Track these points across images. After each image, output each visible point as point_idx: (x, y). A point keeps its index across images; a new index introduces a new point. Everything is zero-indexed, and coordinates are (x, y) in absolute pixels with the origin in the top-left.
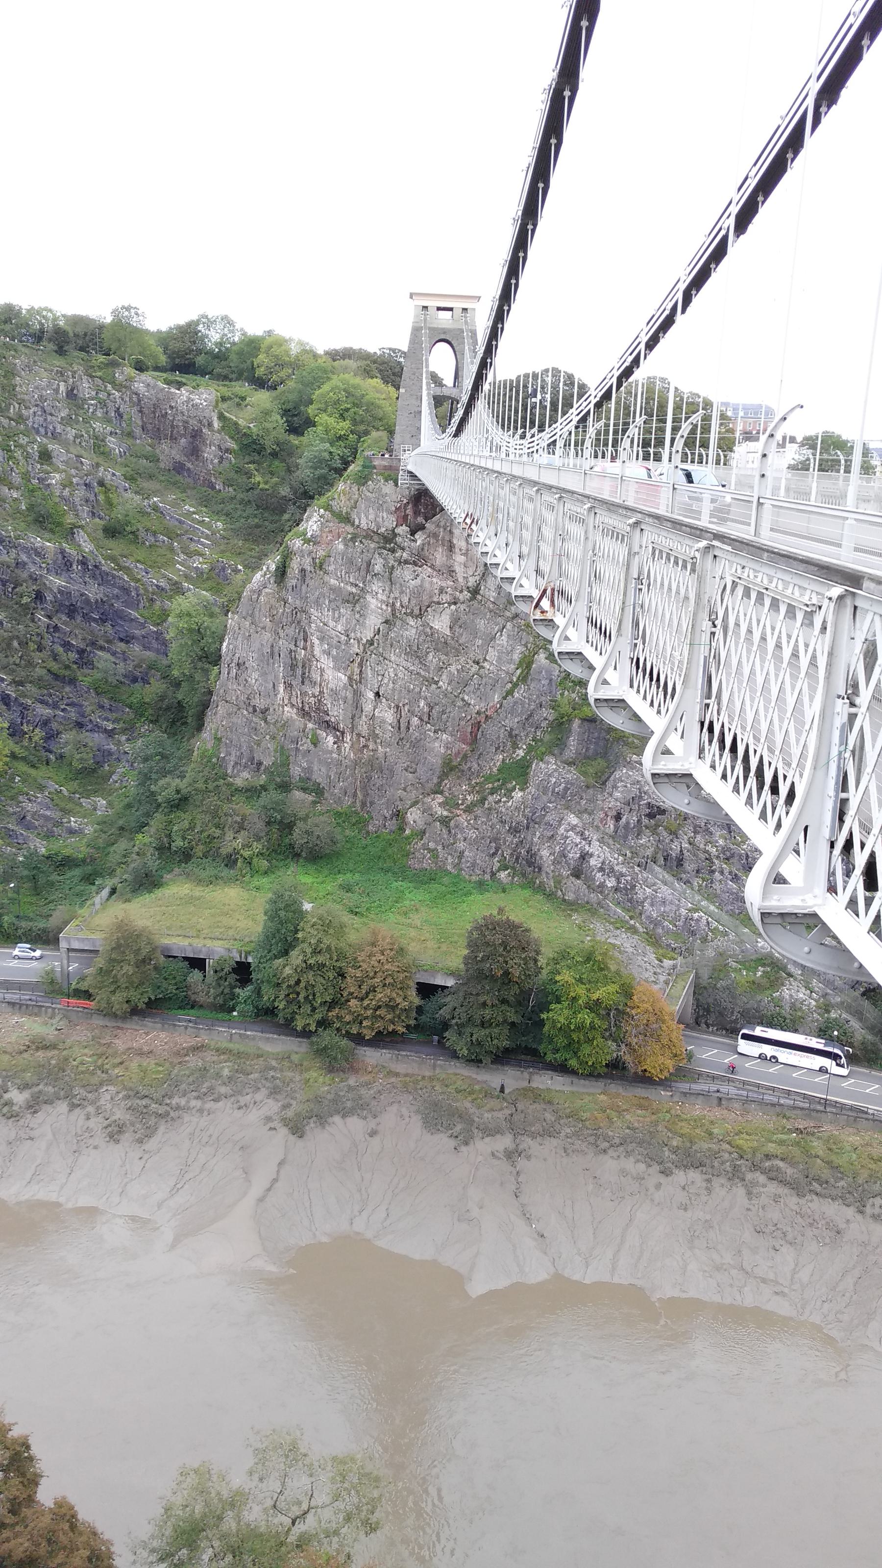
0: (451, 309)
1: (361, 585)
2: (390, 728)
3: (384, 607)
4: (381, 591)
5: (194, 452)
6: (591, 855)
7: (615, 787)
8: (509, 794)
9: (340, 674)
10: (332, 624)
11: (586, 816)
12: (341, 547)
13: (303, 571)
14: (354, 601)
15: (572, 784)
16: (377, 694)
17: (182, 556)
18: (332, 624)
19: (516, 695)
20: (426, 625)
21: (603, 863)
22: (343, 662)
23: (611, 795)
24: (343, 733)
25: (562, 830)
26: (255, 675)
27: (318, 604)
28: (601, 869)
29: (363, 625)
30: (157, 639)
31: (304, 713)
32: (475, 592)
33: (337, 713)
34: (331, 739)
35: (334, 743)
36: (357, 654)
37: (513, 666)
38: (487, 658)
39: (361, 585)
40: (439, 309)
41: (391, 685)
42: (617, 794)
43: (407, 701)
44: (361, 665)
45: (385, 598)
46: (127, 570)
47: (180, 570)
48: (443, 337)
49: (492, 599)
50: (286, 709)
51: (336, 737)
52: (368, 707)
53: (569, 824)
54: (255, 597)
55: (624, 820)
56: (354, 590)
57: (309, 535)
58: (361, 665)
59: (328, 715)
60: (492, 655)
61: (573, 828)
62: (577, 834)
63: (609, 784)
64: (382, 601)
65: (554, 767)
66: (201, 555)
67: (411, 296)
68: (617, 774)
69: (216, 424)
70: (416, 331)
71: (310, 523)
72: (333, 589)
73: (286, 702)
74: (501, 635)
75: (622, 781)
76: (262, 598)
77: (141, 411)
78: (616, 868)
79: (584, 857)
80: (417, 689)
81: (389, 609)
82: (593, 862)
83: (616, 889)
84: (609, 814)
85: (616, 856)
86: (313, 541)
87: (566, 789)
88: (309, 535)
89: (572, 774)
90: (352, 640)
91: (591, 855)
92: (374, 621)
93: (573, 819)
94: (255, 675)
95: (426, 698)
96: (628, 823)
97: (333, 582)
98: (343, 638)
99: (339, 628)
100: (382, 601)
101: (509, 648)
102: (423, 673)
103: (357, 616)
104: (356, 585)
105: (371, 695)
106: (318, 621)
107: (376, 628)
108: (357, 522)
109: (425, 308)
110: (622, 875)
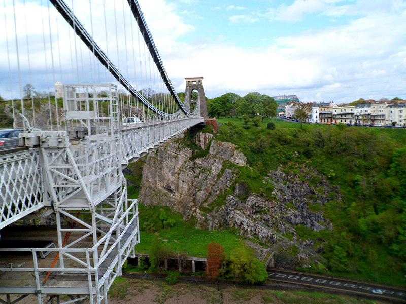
10: (170, 163)
13: (161, 151)
14: (175, 157)
16: (183, 181)
18: (170, 163)
22: (173, 174)
27: (166, 158)
31: (164, 188)
33: (173, 187)
34: (172, 195)
42: (249, 204)
52: (181, 185)
67: (186, 78)
72: (170, 155)
82: (244, 223)
83: (251, 231)
87: (236, 204)
92: (181, 162)
93: (238, 212)
94: (151, 179)
105: (181, 182)
110: (252, 226)
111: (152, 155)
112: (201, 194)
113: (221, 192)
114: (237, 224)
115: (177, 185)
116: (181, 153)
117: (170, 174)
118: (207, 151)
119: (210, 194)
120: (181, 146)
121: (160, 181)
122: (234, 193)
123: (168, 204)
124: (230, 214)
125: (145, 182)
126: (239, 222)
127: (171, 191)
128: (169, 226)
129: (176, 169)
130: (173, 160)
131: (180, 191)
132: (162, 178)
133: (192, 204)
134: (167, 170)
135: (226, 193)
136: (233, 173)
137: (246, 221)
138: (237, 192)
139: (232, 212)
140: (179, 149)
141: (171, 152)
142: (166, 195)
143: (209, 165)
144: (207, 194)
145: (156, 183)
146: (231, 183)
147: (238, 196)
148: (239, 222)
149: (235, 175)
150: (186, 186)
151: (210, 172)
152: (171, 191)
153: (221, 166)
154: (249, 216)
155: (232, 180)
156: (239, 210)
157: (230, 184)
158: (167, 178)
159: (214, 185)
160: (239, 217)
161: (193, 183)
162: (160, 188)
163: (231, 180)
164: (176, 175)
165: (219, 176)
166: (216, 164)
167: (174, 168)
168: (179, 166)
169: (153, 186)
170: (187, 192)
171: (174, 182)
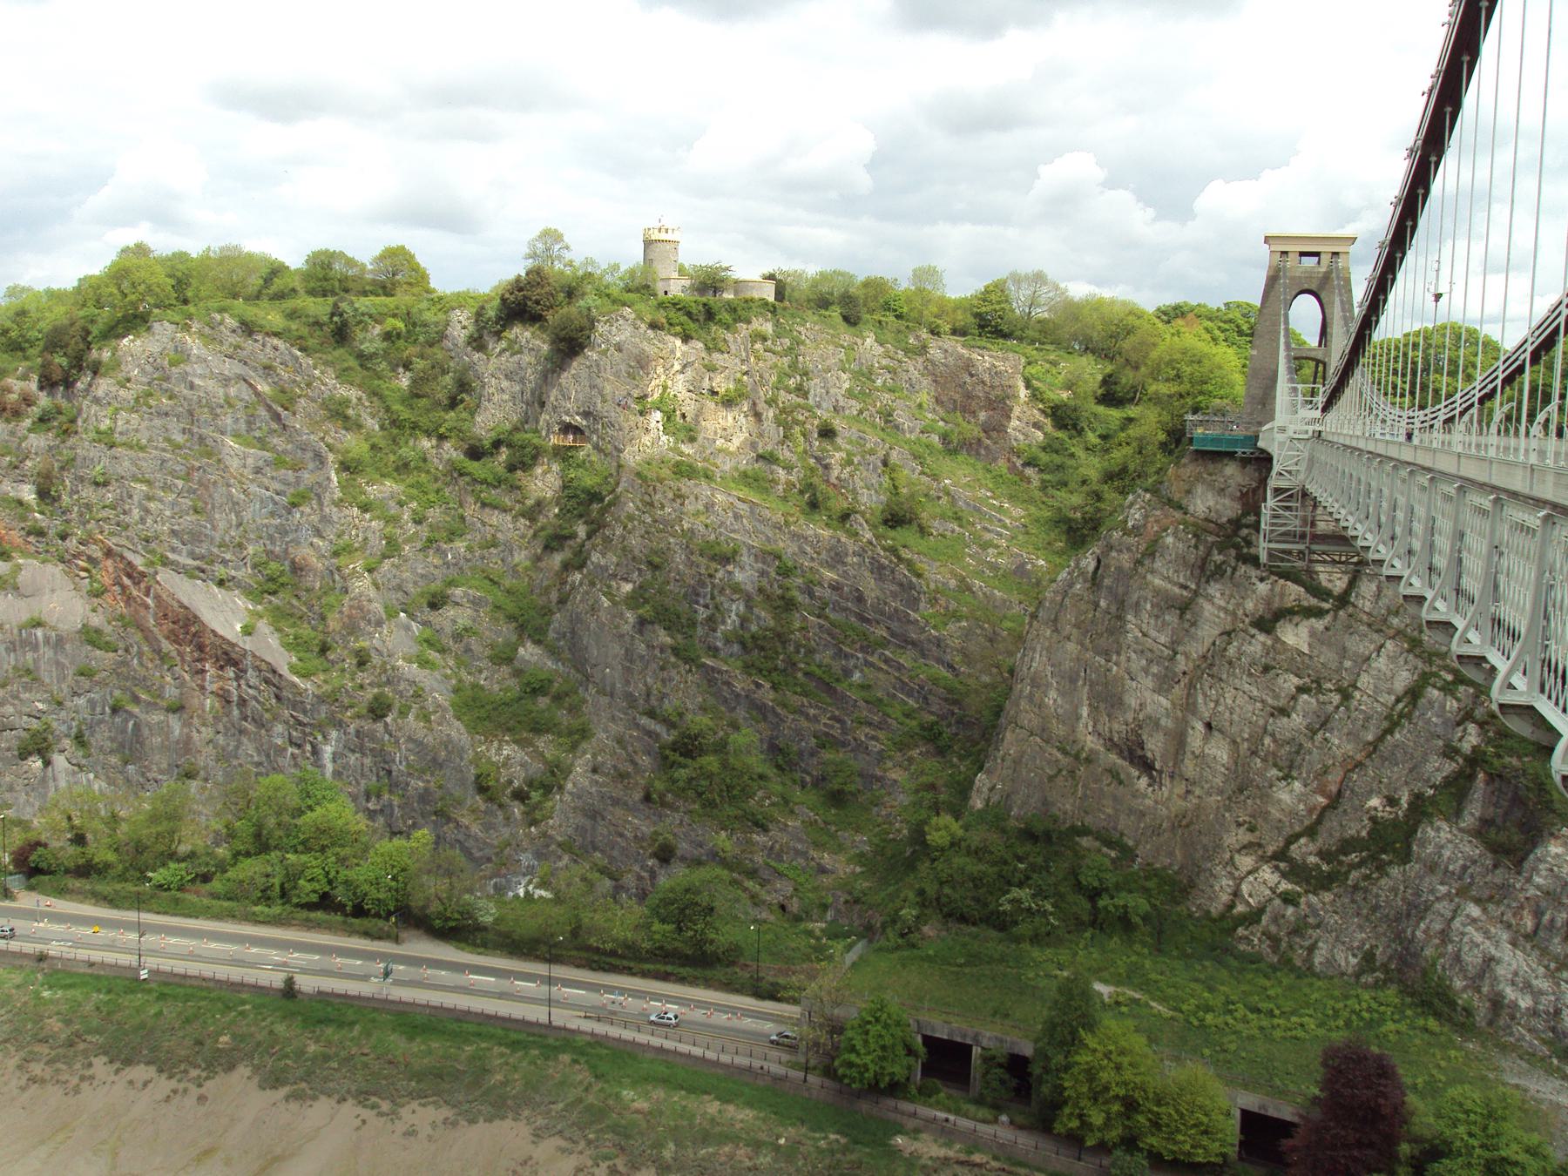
0: (1317, 254)
1: (1193, 586)
2: (1223, 770)
3: (1222, 615)
4: (1218, 595)
5: (995, 429)
6: (1498, 962)
7: (1535, 869)
8: (1381, 868)
9: (1161, 698)
10: (1153, 633)
11: (1491, 907)
12: (1170, 540)
14: (1184, 608)
15: (1474, 862)
16: (1209, 726)
17: (975, 548)
19: (1397, 736)
20: (1278, 640)
21: (1516, 974)
22: (1165, 683)
23: (1529, 880)
24: (1160, 772)
25: (1456, 924)
26: (1053, 694)
27: (1137, 607)
28: (1513, 984)
29: (1193, 638)
30: (939, 646)
31: (1111, 744)
32: (1343, 600)
33: (1155, 746)
34: (1143, 782)
35: (1150, 785)
36: (1184, 673)
37: (1393, 698)
38: (1359, 685)
39: (1193, 586)
40: (1302, 254)
41: (1227, 714)
42: (1537, 880)
43: (1246, 736)
44: (1191, 686)
45: (1222, 603)
46: (909, 564)
47: (970, 565)
48: (1306, 286)
49: (1367, 610)
50: (1089, 738)
51: (1151, 777)
53: (1468, 916)
54: (1059, 598)
55: (1547, 917)
56: (1185, 593)
57: (1130, 524)
58: (1191, 686)
59: (1143, 749)
60: (1364, 681)
61: (1474, 921)
62: (1477, 930)
63: (1526, 865)
64: (1220, 608)
65: (1449, 836)
66: (997, 547)
67: (1267, 240)
68: (1539, 852)
69: (1023, 393)
70: (1272, 281)
71: (1132, 511)
72: (1157, 592)
73: (1090, 729)
74: (1378, 656)
75: (1546, 862)
76: (1067, 601)
77: (935, 381)
78: (1535, 982)
79: (1489, 961)
80: (1261, 722)
81: (1229, 618)
82: (1500, 971)
83: (1534, 1013)
84: (1526, 904)
85: (1534, 966)
86: (1136, 531)
87: (1464, 868)
88: (1130, 524)
89: (1471, 849)
90: (1178, 656)
91: (1498, 962)
92: (1208, 632)
93: (1474, 911)
94: (1053, 694)
95: (1273, 735)
96: (1552, 920)
97: (1157, 582)
98: (1167, 652)
99: (1162, 639)
100: (1220, 608)
101: (1389, 674)
102: (1270, 701)
103: (1186, 625)
104: (1185, 587)
105: (1200, 726)
106: (1136, 630)
107: (1211, 640)
108: (1191, 509)
109: (1284, 253)
110: (1541, 993)
111: (1071, 585)
112: (1290, 796)
113: (1392, 801)
114: (1463, 970)
115: (1179, 740)
116: (1214, 589)
117: (1149, 682)
118: (1343, 600)
119: (1335, 801)
120: (1218, 558)
121: (1094, 709)
122: (1458, 813)
123: (1124, 823)
124: (1429, 916)
125: (1023, 704)
126: (1472, 959)
127: (1147, 766)
128: (1125, 923)
129: (1182, 664)
130: (1171, 618)
131: (1189, 768)
132: (1108, 698)
133: (1244, 836)
134: (1137, 663)
135: (1420, 809)
136: (1467, 716)
137: (1513, 961)
138: (1474, 810)
139: (1444, 907)
140: (1206, 572)
141: (1164, 577)
142: (1114, 774)
143: (1348, 664)
144: (1322, 800)
145: (1078, 718)
146: (1449, 767)
147: (1482, 831)
148: (1472, 959)
149: (1472, 728)
150: (1220, 752)
151: (1346, 696)
152: (1147, 766)
153: (1403, 679)
154: (1527, 937)
155: (1457, 751)
156: (1478, 901)
157: (1439, 769)
158: (1133, 702)
159: (1359, 765)
160: (1478, 937)
161: (1255, 740)
162: (1091, 742)
163: (1450, 752)
164: (1178, 691)
165: (1393, 724)
166: (1381, 663)
167: (1172, 659)
168: (1196, 649)
169: (1059, 730)
170: (1218, 781)
171: (1163, 722)
